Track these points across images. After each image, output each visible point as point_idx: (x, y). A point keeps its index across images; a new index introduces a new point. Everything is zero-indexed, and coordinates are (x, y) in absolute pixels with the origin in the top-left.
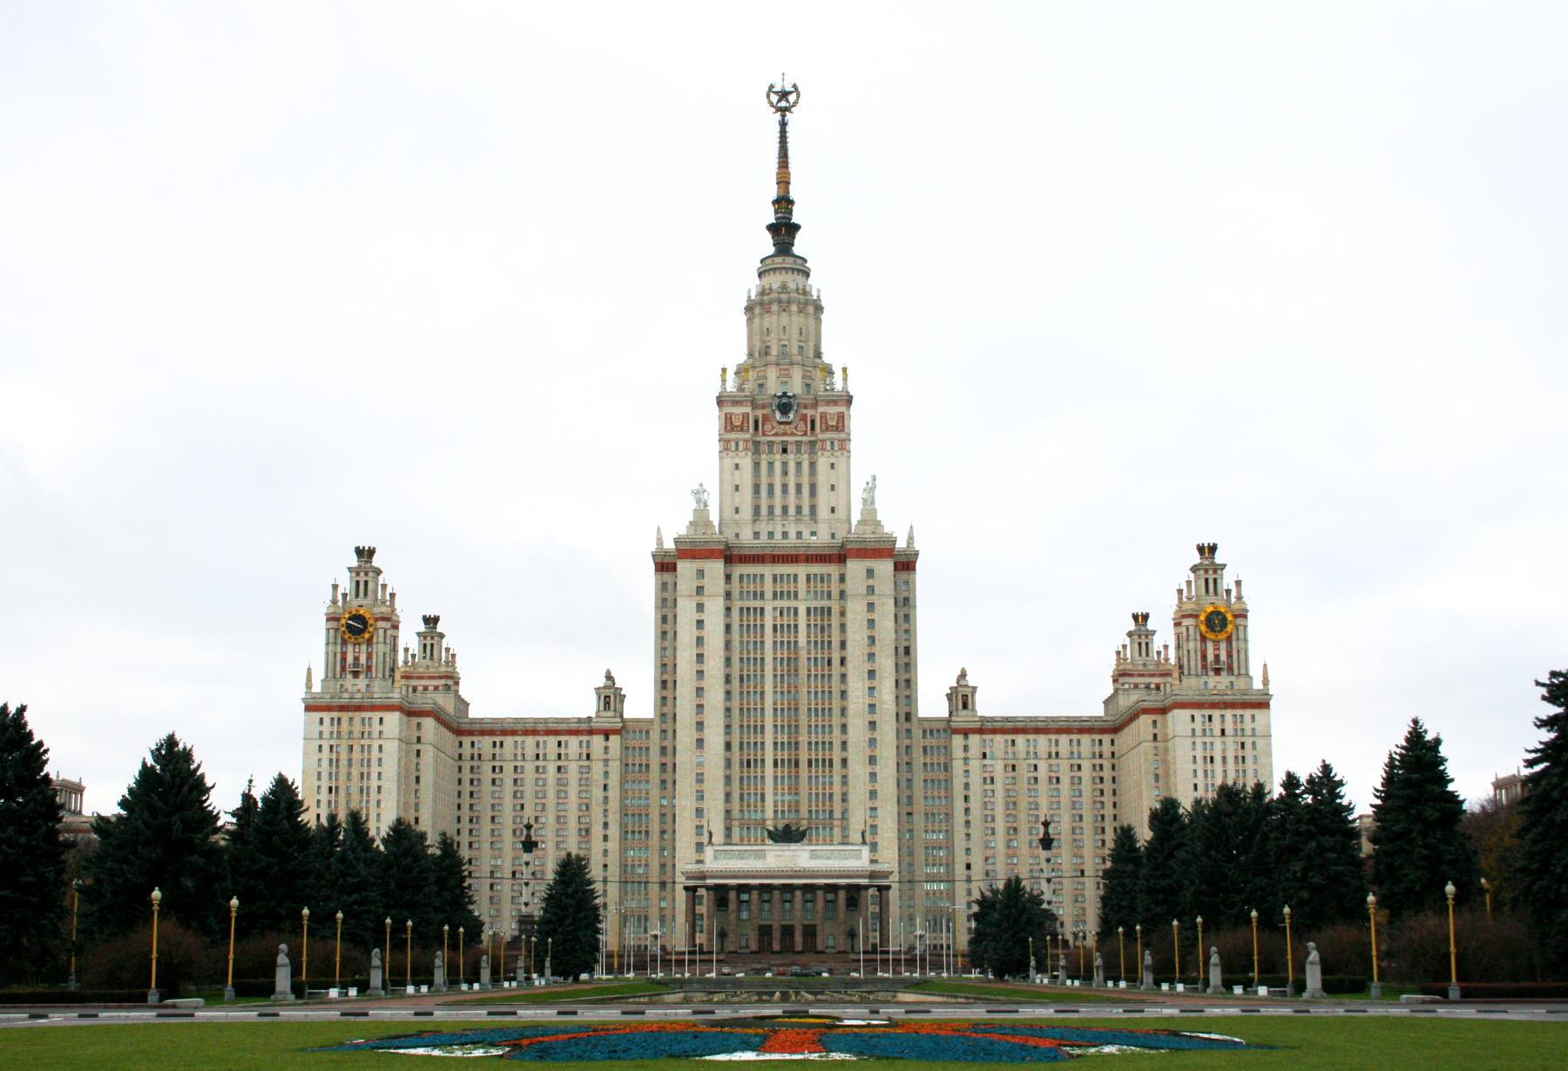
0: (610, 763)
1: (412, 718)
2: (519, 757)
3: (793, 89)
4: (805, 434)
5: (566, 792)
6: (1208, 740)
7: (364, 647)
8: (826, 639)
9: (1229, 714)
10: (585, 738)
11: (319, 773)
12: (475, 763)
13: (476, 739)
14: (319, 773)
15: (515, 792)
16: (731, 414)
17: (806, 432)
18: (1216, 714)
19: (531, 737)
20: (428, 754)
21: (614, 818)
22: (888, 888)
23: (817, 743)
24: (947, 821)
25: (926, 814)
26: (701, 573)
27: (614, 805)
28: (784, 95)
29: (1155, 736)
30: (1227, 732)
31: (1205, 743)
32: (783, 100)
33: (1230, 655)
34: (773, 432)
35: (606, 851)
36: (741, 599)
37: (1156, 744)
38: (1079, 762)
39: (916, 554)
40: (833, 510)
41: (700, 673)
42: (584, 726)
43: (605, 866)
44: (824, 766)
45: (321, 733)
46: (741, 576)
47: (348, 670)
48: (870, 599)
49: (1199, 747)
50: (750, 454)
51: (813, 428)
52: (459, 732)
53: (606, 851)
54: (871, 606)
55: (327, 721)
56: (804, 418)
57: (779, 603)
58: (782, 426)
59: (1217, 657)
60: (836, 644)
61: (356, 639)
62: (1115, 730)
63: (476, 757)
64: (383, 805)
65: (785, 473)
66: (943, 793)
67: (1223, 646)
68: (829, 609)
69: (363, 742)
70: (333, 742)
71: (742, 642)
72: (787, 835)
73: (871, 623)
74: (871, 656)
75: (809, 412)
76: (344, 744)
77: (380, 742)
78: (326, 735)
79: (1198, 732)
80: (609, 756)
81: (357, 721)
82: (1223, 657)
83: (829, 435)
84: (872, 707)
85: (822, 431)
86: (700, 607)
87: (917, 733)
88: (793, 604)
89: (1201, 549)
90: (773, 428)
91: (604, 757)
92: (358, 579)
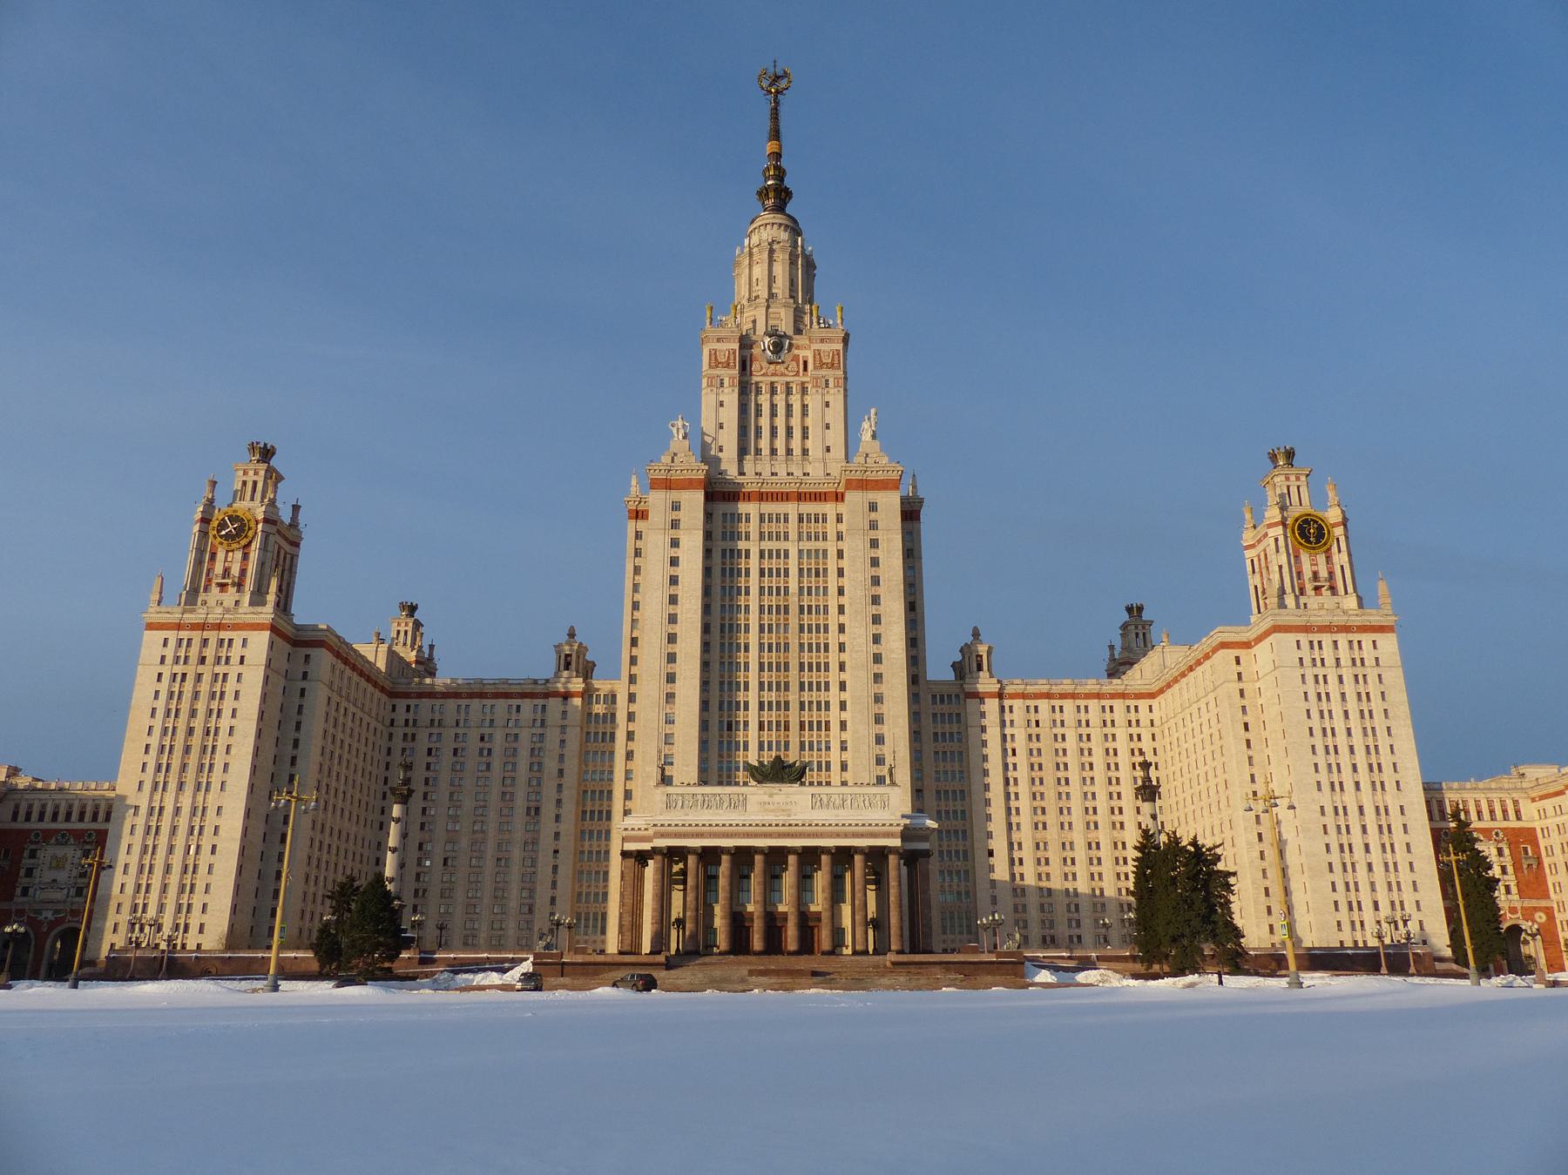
0: (568, 730)
1: (299, 649)
2: (461, 724)
3: (779, 72)
4: (797, 374)
5: (514, 764)
6: (1320, 671)
7: (239, 555)
8: (821, 585)
9: (1342, 639)
10: (540, 702)
11: (154, 710)
12: (409, 731)
13: (412, 702)
14: (154, 710)
15: (504, 793)
16: (716, 350)
17: (798, 372)
18: (1327, 639)
19: (477, 700)
20: (319, 697)
21: (569, 795)
22: (926, 854)
23: (810, 703)
24: (963, 799)
25: (938, 792)
26: (676, 507)
27: (570, 780)
28: (777, 78)
29: (1239, 674)
30: (1342, 662)
31: (1316, 676)
32: (776, 83)
33: (1331, 574)
34: (762, 373)
35: (557, 835)
36: (724, 539)
37: (1241, 685)
38: (1113, 730)
39: (921, 501)
40: (828, 450)
41: (673, 619)
42: (539, 689)
43: (556, 852)
44: (819, 729)
45: (163, 658)
46: (725, 515)
47: (214, 581)
48: (873, 534)
49: (1310, 680)
50: (737, 390)
51: (805, 369)
52: (393, 695)
53: (557, 835)
54: (874, 544)
55: (172, 643)
56: (796, 358)
57: (767, 545)
58: (772, 366)
59: (1315, 575)
60: (833, 590)
61: (229, 545)
62: (1152, 696)
63: (411, 722)
64: (233, 751)
65: (773, 414)
66: (957, 768)
67: (1321, 559)
68: (825, 552)
69: (218, 669)
70: (179, 669)
71: (723, 588)
72: (780, 772)
73: (875, 562)
74: (876, 600)
75: (802, 353)
76: (191, 670)
77: (240, 669)
78: (169, 660)
79: (1307, 661)
80: (566, 722)
81: (213, 643)
82: (1323, 574)
83: (824, 372)
84: (877, 659)
85: (815, 368)
86: (675, 543)
87: (926, 698)
88: (782, 545)
89: (1129, 609)
90: (762, 368)
91: (561, 722)
92: (399, 628)
